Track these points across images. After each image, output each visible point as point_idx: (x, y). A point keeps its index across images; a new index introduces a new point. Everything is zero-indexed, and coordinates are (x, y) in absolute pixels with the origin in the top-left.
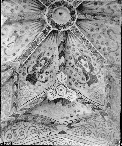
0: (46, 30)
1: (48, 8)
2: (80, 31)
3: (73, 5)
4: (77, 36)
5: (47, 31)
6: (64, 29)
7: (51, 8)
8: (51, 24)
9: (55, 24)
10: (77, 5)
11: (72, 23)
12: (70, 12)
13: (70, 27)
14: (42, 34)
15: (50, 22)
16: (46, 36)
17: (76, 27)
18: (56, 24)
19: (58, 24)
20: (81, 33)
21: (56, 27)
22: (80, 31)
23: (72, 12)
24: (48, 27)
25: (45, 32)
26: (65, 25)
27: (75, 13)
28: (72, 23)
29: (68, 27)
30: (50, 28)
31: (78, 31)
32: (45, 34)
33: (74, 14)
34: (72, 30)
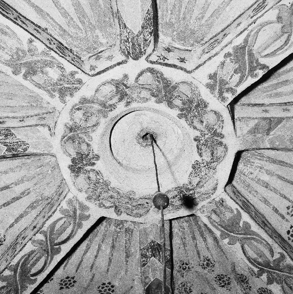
0: (237, 77)
1: (215, 189)
2: (20, 78)
3: (83, 208)
4: (31, 41)
5: (231, 66)
6: (126, 76)
7: (202, 190)
8: (206, 106)
9: (178, 102)
10: (62, 212)
11: (79, 115)
12: (95, 167)
13: (86, 91)
14: (267, 56)
15: (210, 118)
16: (246, 41)
17: (52, 96)
18: (170, 105)
19: (159, 102)
20: (9, 70)
21: (175, 88)
22: (20, 78)
23: (89, 168)
24: (221, 93)
25: (251, 62)
26: (121, 100)
27: (70, 167)
28: (79, 115)
29: (97, 91)
30: (211, 87)
31: (34, 78)
32: (251, 55)
33: (73, 160)
34: (72, 74)
